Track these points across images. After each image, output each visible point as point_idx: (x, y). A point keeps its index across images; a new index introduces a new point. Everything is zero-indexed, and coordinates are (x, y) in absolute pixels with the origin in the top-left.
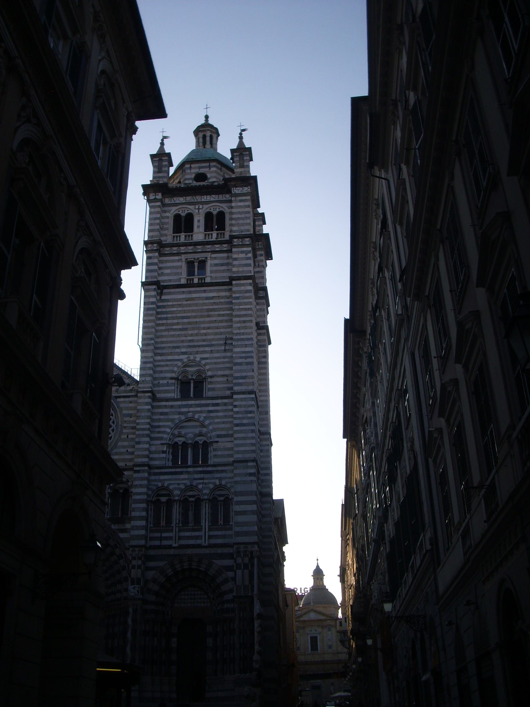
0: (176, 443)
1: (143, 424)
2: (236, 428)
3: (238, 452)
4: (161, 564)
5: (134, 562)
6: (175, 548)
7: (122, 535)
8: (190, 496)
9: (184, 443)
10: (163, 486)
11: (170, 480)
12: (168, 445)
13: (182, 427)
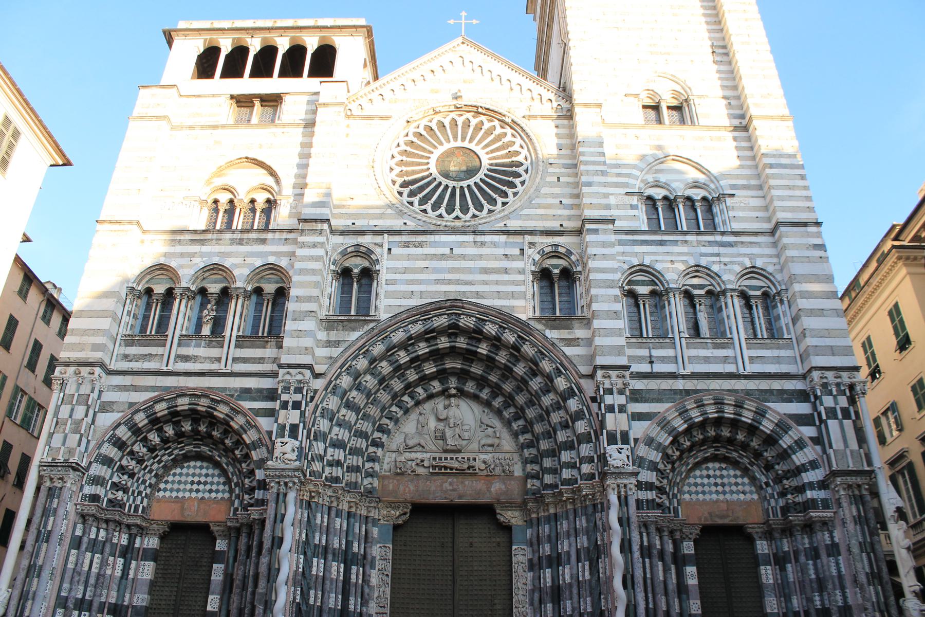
0: (649, 198)
2: (768, 171)
3: (785, 209)
5: (609, 400)
6: (684, 377)
7: (569, 351)
9: (665, 198)
12: (640, 194)
13: (657, 171)
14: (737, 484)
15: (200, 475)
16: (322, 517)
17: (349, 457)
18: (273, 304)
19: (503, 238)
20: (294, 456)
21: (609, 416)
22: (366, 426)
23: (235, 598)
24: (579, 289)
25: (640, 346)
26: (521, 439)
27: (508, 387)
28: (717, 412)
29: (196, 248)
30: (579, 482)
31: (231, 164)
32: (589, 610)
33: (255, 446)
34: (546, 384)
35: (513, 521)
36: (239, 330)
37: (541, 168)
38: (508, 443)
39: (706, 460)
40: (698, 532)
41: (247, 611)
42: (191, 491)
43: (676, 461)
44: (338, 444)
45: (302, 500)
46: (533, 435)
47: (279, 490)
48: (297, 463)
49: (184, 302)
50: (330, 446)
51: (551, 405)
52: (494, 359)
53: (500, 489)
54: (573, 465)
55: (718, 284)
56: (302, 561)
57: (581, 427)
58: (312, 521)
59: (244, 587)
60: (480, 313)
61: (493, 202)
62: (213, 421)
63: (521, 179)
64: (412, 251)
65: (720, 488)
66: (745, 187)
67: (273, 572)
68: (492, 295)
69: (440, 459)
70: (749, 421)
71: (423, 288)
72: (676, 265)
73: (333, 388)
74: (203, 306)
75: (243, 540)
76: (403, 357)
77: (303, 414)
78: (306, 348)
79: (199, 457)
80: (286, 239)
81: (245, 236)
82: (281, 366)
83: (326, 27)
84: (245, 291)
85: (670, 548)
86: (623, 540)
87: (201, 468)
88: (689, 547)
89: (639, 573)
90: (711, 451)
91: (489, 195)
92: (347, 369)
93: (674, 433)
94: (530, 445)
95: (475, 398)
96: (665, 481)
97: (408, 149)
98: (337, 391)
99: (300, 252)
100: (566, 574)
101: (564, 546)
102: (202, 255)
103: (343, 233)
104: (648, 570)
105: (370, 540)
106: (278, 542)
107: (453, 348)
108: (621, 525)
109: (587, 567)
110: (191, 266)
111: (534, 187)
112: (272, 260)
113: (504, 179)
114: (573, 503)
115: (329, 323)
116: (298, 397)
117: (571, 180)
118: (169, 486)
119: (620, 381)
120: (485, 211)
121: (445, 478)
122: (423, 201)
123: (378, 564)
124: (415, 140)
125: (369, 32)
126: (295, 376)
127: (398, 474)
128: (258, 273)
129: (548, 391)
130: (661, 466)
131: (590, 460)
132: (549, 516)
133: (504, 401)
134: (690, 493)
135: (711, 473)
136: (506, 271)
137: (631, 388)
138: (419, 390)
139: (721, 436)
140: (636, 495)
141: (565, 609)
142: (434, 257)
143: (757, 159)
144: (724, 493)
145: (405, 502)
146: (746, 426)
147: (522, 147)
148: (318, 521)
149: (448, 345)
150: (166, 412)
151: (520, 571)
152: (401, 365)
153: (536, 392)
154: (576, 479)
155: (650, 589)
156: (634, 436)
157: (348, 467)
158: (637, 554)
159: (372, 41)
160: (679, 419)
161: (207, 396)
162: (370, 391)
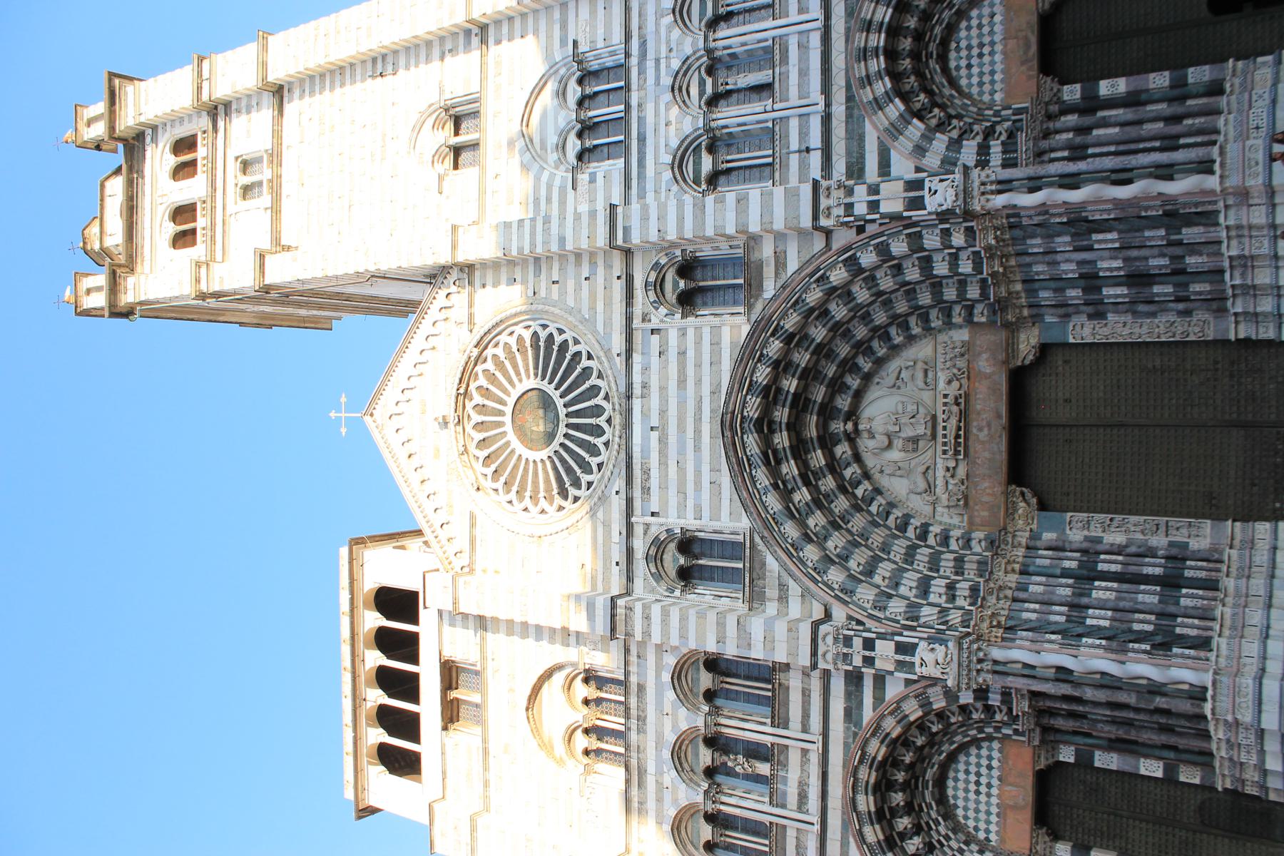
0: (580, 157)
1: (521, 237)
5: (861, 209)
6: (828, 104)
7: (792, 265)
8: (702, 92)
9: (580, 135)
10: (673, 169)
11: (656, 148)
13: (543, 147)
14: (980, 26)
15: (967, 782)
16: (1028, 610)
17: (941, 573)
18: (728, 675)
19: (637, 358)
20: (940, 650)
21: (884, 208)
22: (899, 547)
23: (1145, 736)
24: (706, 252)
25: (785, 166)
26: (916, 330)
27: (844, 350)
28: (877, 57)
29: (650, 781)
30: (977, 249)
31: (536, 731)
32: (1162, 232)
33: (925, 704)
34: (839, 296)
35: (1034, 341)
36: (764, 724)
37: (540, 307)
38: (923, 350)
39: (945, 70)
40: (1049, 79)
41: (1163, 721)
42: (989, 795)
43: (946, 113)
44: (924, 587)
45: (1003, 639)
46: (912, 314)
47: (988, 671)
48: (950, 644)
49: (724, 799)
50: (926, 599)
51: (869, 289)
52: (805, 369)
53: (987, 360)
54: (953, 255)
55: (698, 59)
56: (1090, 641)
57: (899, 247)
58: (1033, 625)
59: (1129, 723)
60: (740, 389)
61: (587, 372)
62: (890, 762)
63: (556, 334)
64: (654, 483)
65: (986, 50)
66: (564, 26)
67: (1106, 681)
68: (716, 372)
69: (945, 444)
70: (890, 11)
71: (706, 469)
72: (672, 118)
73: (846, 594)
74: (730, 773)
75: (1059, 723)
76: (802, 496)
77: (882, 636)
78: (790, 630)
79: (941, 782)
80: (639, 657)
81: (634, 712)
82: (814, 666)
83: (352, 600)
84: (709, 714)
85: (1072, 119)
86: (1062, 186)
87: (956, 780)
88: (1071, 92)
89: (1109, 163)
90: (932, 63)
91: (577, 377)
92: (818, 573)
93: (907, 116)
94: (925, 318)
95: (858, 395)
96: (976, 128)
97: (515, 488)
98: (849, 587)
99: (656, 638)
100: (1109, 265)
101: (1069, 269)
102: (660, 773)
103: (630, 578)
104: (1105, 149)
105: (1060, 544)
106: (1063, 674)
107: (790, 427)
108: (1039, 189)
109: (1100, 236)
110: (675, 792)
111: (566, 316)
112: (666, 677)
113: (555, 357)
114: (1007, 256)
115: (755, 598)
116: (857, 643)
117: (556, 266)
118: (982, 825)
119: (835, 194)
120: (599, 382)
121: (972, 439)
122: (587, 468)
123: (1096, 532)
124: (502, 480)
125: (358, 542)
126: (828, 646)
127: (966, 504)
128: (685, 695)
129: (849, 293)
130: (955, 134)
131: (946, 233)
132: (1026, 291)
133: (864, 354)
134: (992, 93)
135: (963, 63)
136: (682, 353)
137: (844, 178)
138: (848, 473)
139: (911, 51)
140: (996, 170)
141: (1160, 267)
142: (663, 453)
143: (526, 10)
144: (992, 43)
145: (1006, 494)
146: (897, 15)
147: (512, 333)
148: (1033, 616)
149: (785, 433)
150: (877, 827)
151: (1106, 331)
152: (813, 499)
153: (850, 310)
154: (974, 253)
155: (1133, 146)
156: (912, 171)
157: (957, 574)
158: (1081, 166)
159: (369, 537)
160: (887, 110)
161: (856, 769)
162: (849, 541)
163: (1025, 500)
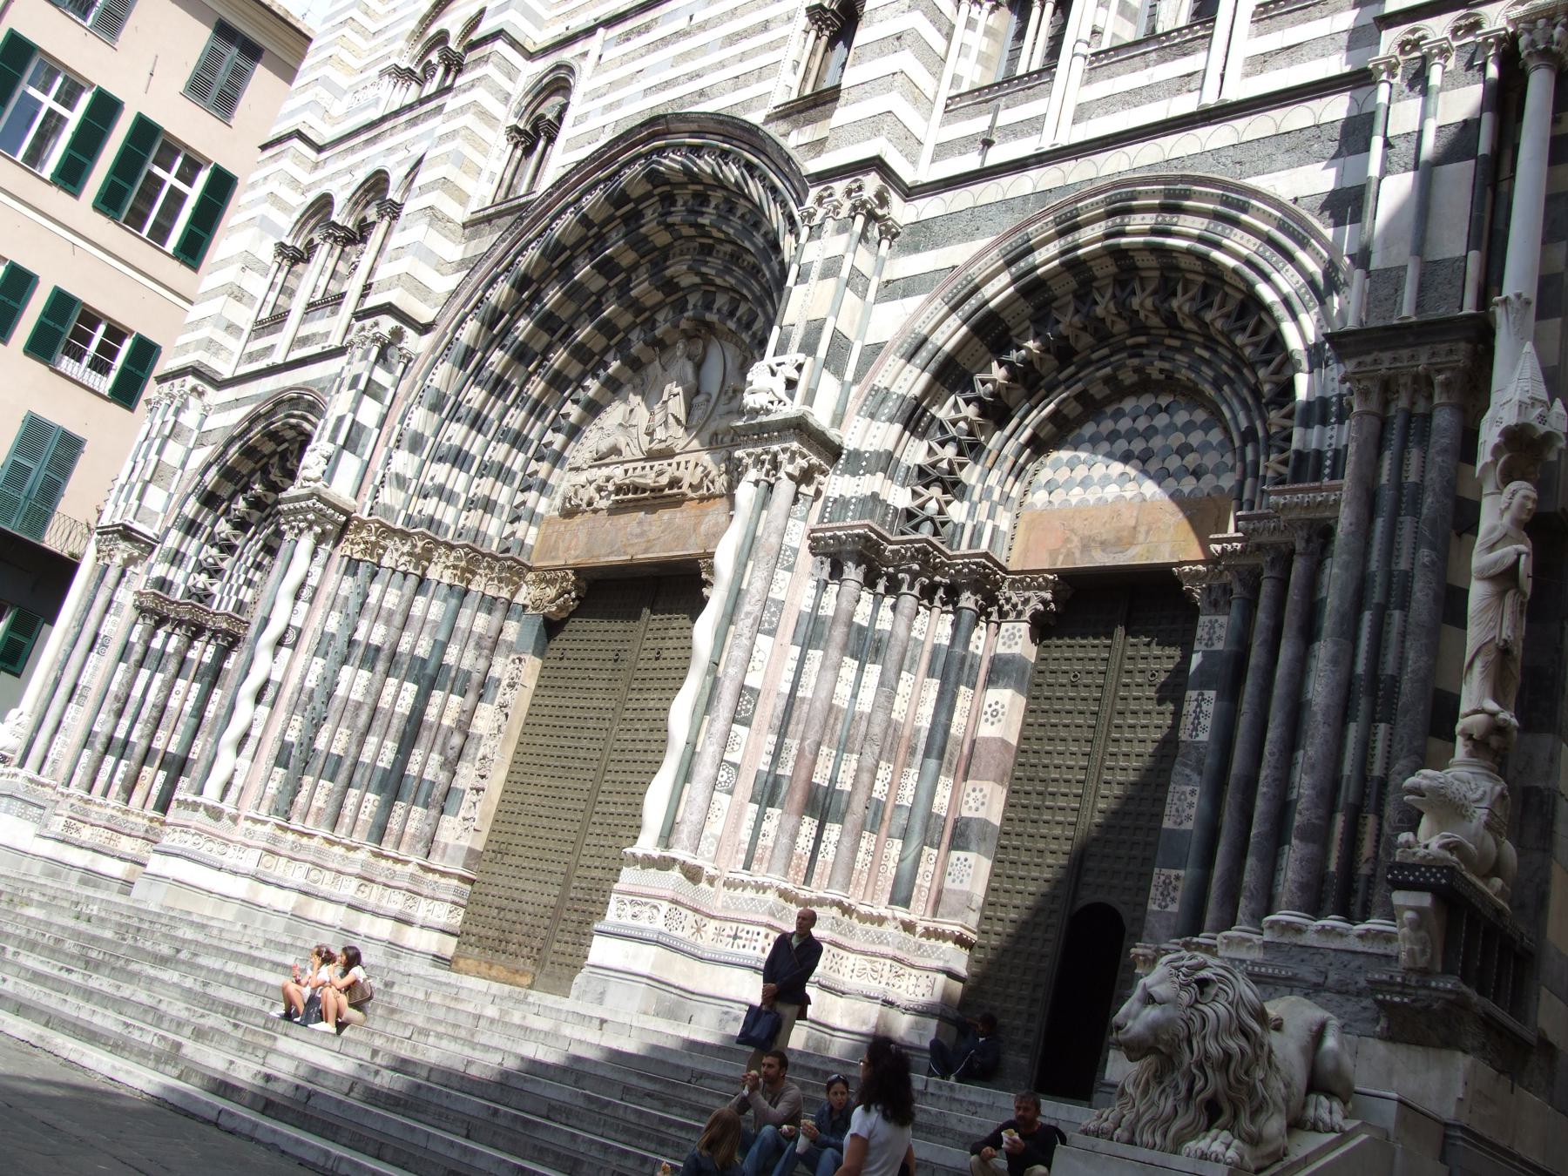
4: (957, 254)
14: (1184, 450)
103: (546, 51)
134: (1050, 487)
136: (765, 26)
148: (373, 600)
163: (560, 595)
